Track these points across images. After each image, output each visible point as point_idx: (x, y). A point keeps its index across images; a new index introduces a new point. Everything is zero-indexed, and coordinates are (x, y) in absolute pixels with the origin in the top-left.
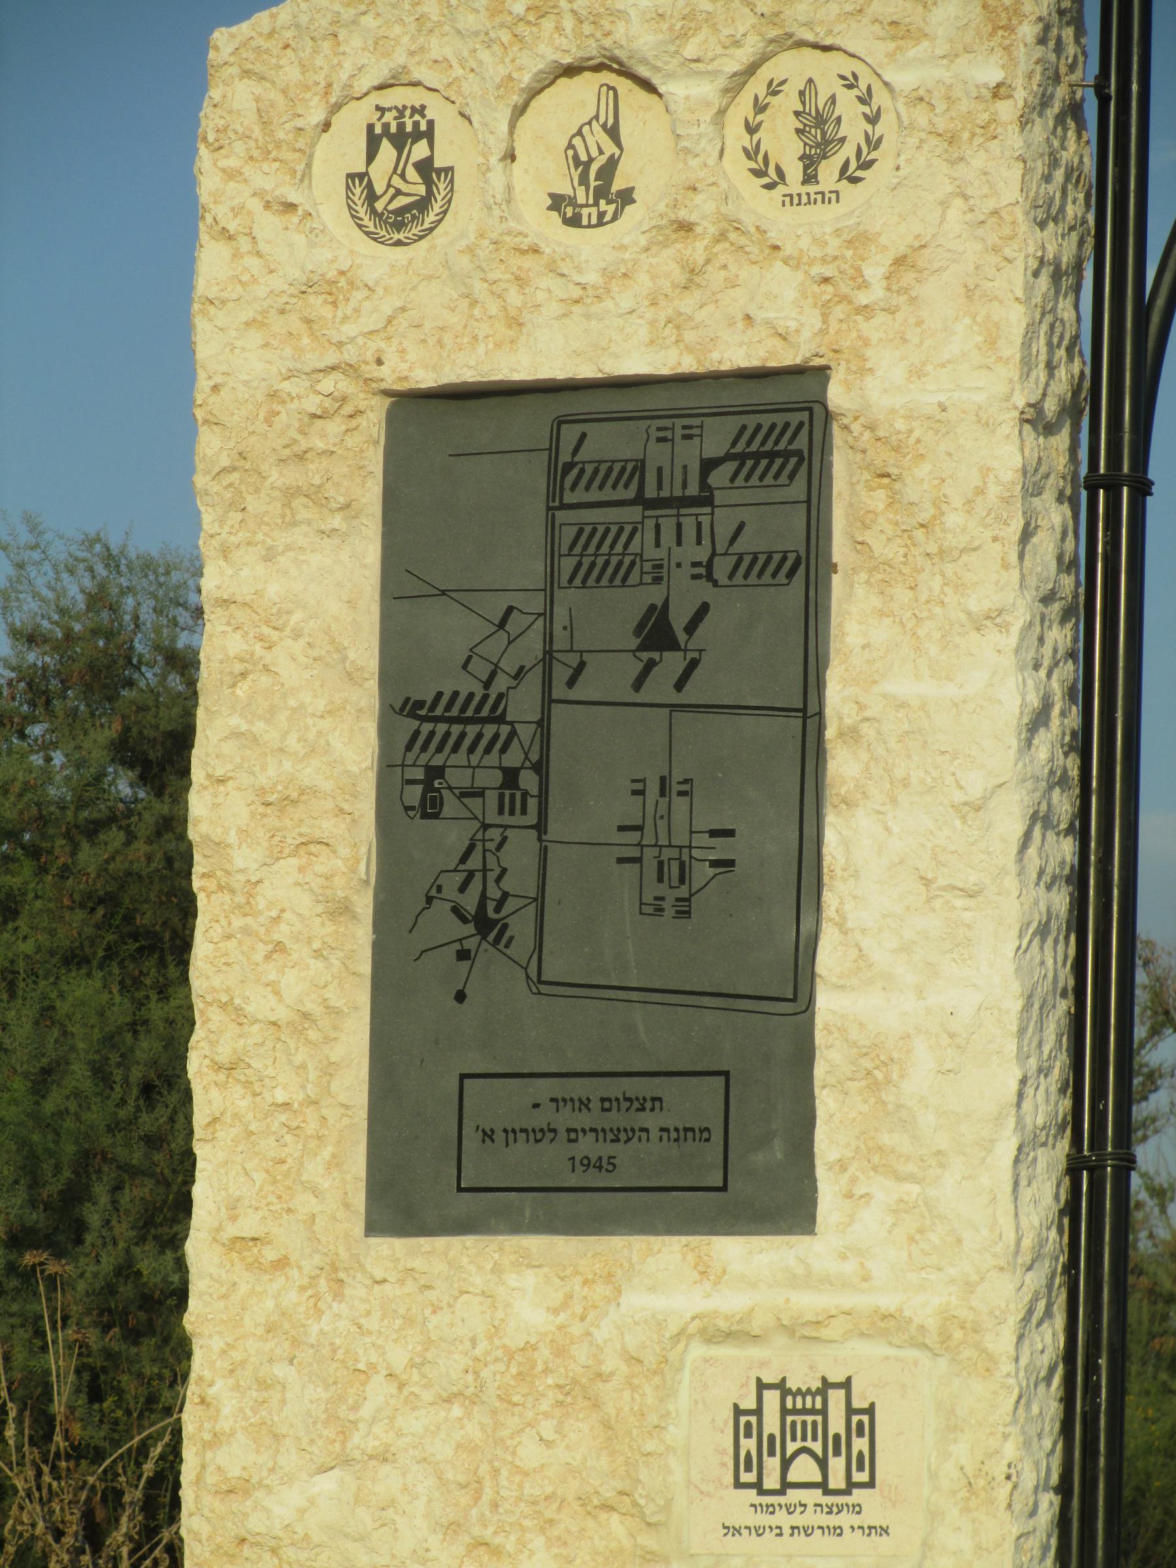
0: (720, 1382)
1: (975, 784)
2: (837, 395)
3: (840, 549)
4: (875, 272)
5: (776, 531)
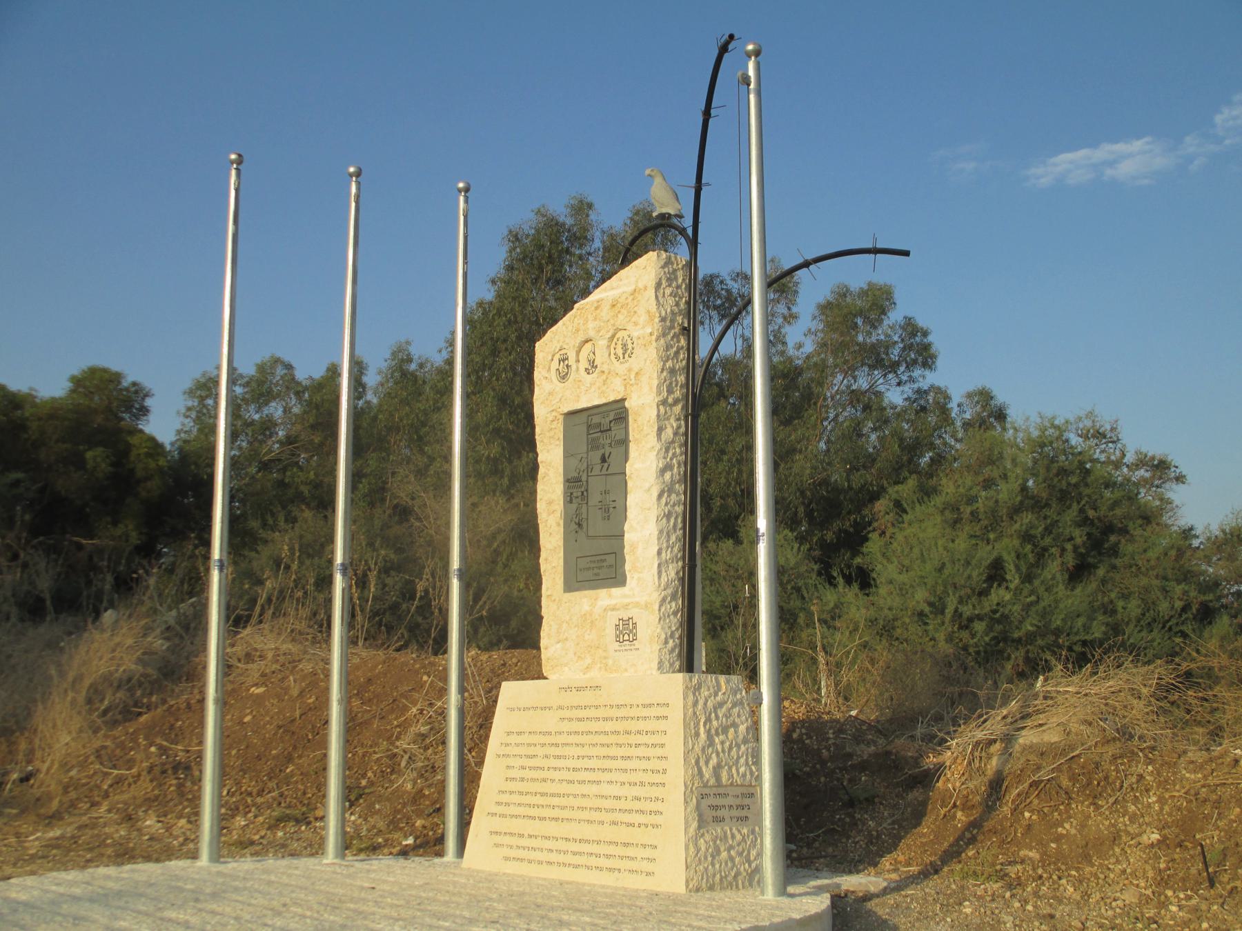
0: (612, 619)
1: (647, 485)
2: (627, 404)
3: (631, 438)
4: (632, 377)
5: (620, 436)
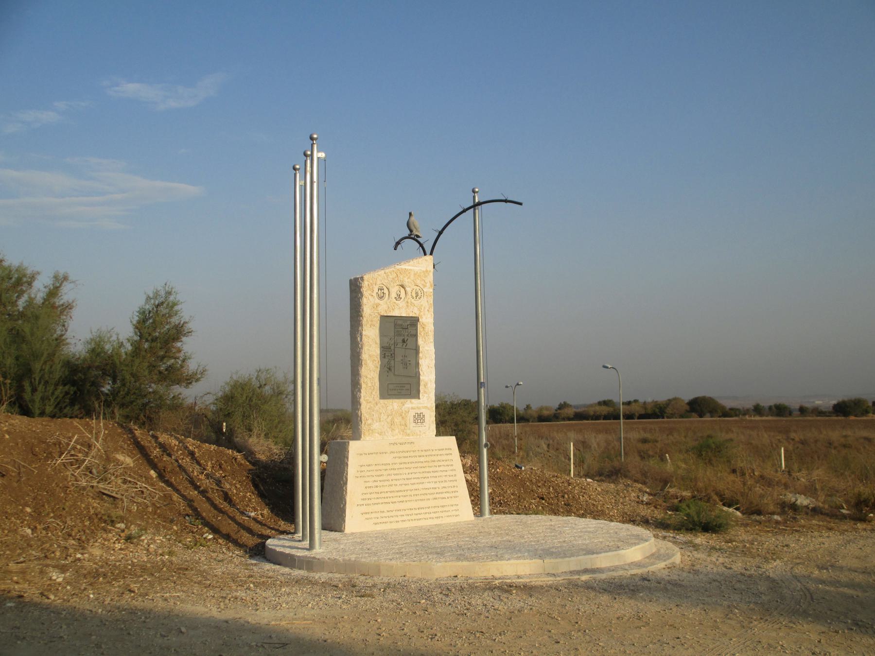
0: (412, 413)
5: (413, 332)
